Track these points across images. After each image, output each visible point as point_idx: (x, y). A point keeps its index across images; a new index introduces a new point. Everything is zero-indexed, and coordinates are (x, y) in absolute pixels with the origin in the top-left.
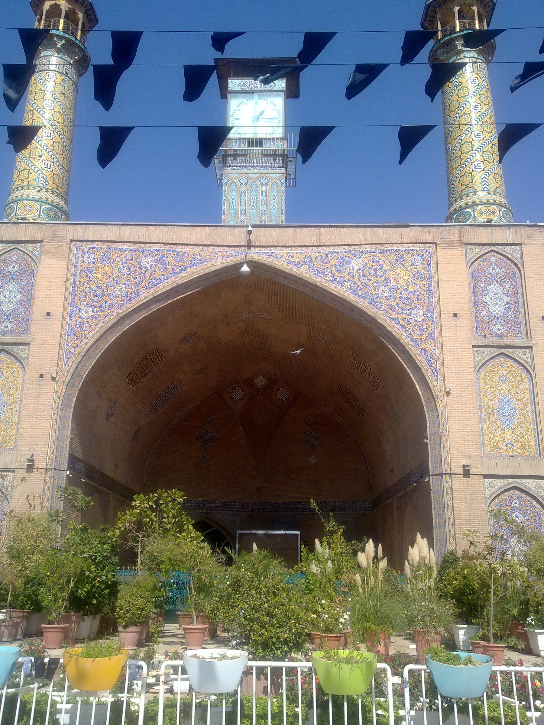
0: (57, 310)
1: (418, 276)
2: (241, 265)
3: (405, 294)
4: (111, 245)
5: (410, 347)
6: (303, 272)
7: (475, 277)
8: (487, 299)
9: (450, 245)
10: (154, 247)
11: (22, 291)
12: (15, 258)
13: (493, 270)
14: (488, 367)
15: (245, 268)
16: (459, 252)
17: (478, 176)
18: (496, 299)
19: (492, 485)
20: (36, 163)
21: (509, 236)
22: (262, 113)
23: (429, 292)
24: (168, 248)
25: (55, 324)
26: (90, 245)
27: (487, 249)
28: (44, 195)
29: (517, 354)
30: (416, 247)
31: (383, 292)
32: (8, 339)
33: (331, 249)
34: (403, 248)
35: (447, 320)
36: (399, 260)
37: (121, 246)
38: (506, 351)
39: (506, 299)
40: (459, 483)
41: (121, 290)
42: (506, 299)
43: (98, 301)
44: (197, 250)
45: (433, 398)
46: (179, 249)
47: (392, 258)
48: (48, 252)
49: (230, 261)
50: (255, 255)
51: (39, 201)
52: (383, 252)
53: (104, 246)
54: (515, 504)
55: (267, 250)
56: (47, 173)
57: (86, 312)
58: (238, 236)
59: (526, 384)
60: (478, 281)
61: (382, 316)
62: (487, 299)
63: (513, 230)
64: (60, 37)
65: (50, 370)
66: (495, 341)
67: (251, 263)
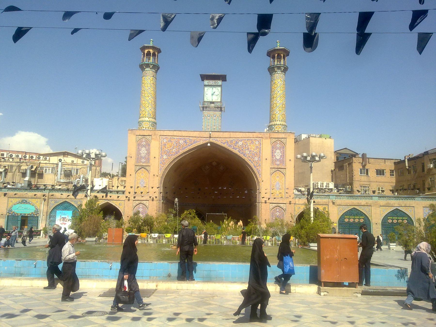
0: (157, 157)
1: (257, 147)
2: (208, 143)
3: (253, 153)
4: (171, 137)
5: (254, 168)
6: (225, 146)
7: (273, 148)
8: (275, 154)
9: (266, 138)
10: (183, 138)
11: (147, 150)
12: (144, 140)
13: (278, 146)
14: (274, 174)
15: (209, 145)
16: (268, 141)
17: (277, 115)
18: (278, 154)
19: (272, 205)
20: (147, 109)
21: (283, 136)
22: (214, 93)
23: (260, 152)
24: (187, 138)
25: (157, 160)
26: (165, 137)
27: (277, 139)
28: (150, 119)
29: (282, 170)
30: (257, 139)
31: (247, 152)
32: (144, 165)
33: (233, 139)
34: (253, 139)
35: (264, 160)
36: (252, 142)
37: (174, 137)
38: (279, 169)
39: (281, 154)
40: (263, 205)
41: (174, 150)
42: (281, 154)
43: (168, 153)
44: (195, 138)
45: (259, 182)
46: (190, 138)
47: (250, 142)
48: (153, 139)
49: (204, 142)
50: (211, 140)
51: (149, 122)
52: (248, 140)
53: (169, 137)
54: (278, 210)
55: (215, 139)
56: (151, 112)
57: (165, 157)
58: (207, 135)
59: (284, 179)
60: (274, 148)
61: (246, 159)
62: (275, 154)
63: (284, 134)
64: (151, 64)
65: (156, 174)
66: (276, 167)
67: (211, 143)
